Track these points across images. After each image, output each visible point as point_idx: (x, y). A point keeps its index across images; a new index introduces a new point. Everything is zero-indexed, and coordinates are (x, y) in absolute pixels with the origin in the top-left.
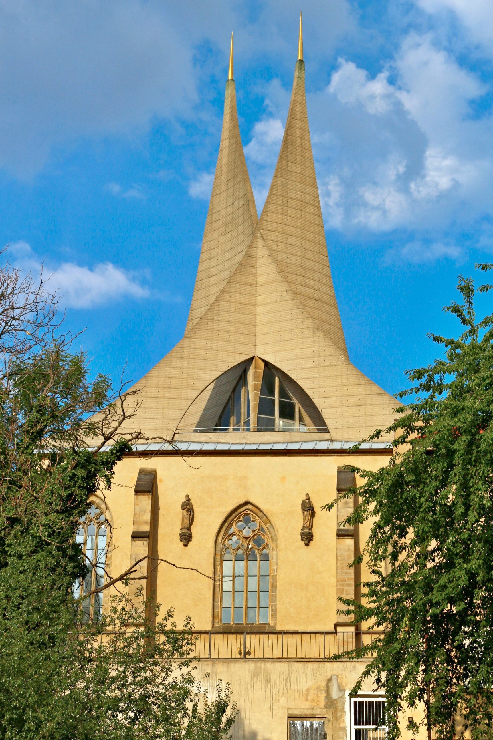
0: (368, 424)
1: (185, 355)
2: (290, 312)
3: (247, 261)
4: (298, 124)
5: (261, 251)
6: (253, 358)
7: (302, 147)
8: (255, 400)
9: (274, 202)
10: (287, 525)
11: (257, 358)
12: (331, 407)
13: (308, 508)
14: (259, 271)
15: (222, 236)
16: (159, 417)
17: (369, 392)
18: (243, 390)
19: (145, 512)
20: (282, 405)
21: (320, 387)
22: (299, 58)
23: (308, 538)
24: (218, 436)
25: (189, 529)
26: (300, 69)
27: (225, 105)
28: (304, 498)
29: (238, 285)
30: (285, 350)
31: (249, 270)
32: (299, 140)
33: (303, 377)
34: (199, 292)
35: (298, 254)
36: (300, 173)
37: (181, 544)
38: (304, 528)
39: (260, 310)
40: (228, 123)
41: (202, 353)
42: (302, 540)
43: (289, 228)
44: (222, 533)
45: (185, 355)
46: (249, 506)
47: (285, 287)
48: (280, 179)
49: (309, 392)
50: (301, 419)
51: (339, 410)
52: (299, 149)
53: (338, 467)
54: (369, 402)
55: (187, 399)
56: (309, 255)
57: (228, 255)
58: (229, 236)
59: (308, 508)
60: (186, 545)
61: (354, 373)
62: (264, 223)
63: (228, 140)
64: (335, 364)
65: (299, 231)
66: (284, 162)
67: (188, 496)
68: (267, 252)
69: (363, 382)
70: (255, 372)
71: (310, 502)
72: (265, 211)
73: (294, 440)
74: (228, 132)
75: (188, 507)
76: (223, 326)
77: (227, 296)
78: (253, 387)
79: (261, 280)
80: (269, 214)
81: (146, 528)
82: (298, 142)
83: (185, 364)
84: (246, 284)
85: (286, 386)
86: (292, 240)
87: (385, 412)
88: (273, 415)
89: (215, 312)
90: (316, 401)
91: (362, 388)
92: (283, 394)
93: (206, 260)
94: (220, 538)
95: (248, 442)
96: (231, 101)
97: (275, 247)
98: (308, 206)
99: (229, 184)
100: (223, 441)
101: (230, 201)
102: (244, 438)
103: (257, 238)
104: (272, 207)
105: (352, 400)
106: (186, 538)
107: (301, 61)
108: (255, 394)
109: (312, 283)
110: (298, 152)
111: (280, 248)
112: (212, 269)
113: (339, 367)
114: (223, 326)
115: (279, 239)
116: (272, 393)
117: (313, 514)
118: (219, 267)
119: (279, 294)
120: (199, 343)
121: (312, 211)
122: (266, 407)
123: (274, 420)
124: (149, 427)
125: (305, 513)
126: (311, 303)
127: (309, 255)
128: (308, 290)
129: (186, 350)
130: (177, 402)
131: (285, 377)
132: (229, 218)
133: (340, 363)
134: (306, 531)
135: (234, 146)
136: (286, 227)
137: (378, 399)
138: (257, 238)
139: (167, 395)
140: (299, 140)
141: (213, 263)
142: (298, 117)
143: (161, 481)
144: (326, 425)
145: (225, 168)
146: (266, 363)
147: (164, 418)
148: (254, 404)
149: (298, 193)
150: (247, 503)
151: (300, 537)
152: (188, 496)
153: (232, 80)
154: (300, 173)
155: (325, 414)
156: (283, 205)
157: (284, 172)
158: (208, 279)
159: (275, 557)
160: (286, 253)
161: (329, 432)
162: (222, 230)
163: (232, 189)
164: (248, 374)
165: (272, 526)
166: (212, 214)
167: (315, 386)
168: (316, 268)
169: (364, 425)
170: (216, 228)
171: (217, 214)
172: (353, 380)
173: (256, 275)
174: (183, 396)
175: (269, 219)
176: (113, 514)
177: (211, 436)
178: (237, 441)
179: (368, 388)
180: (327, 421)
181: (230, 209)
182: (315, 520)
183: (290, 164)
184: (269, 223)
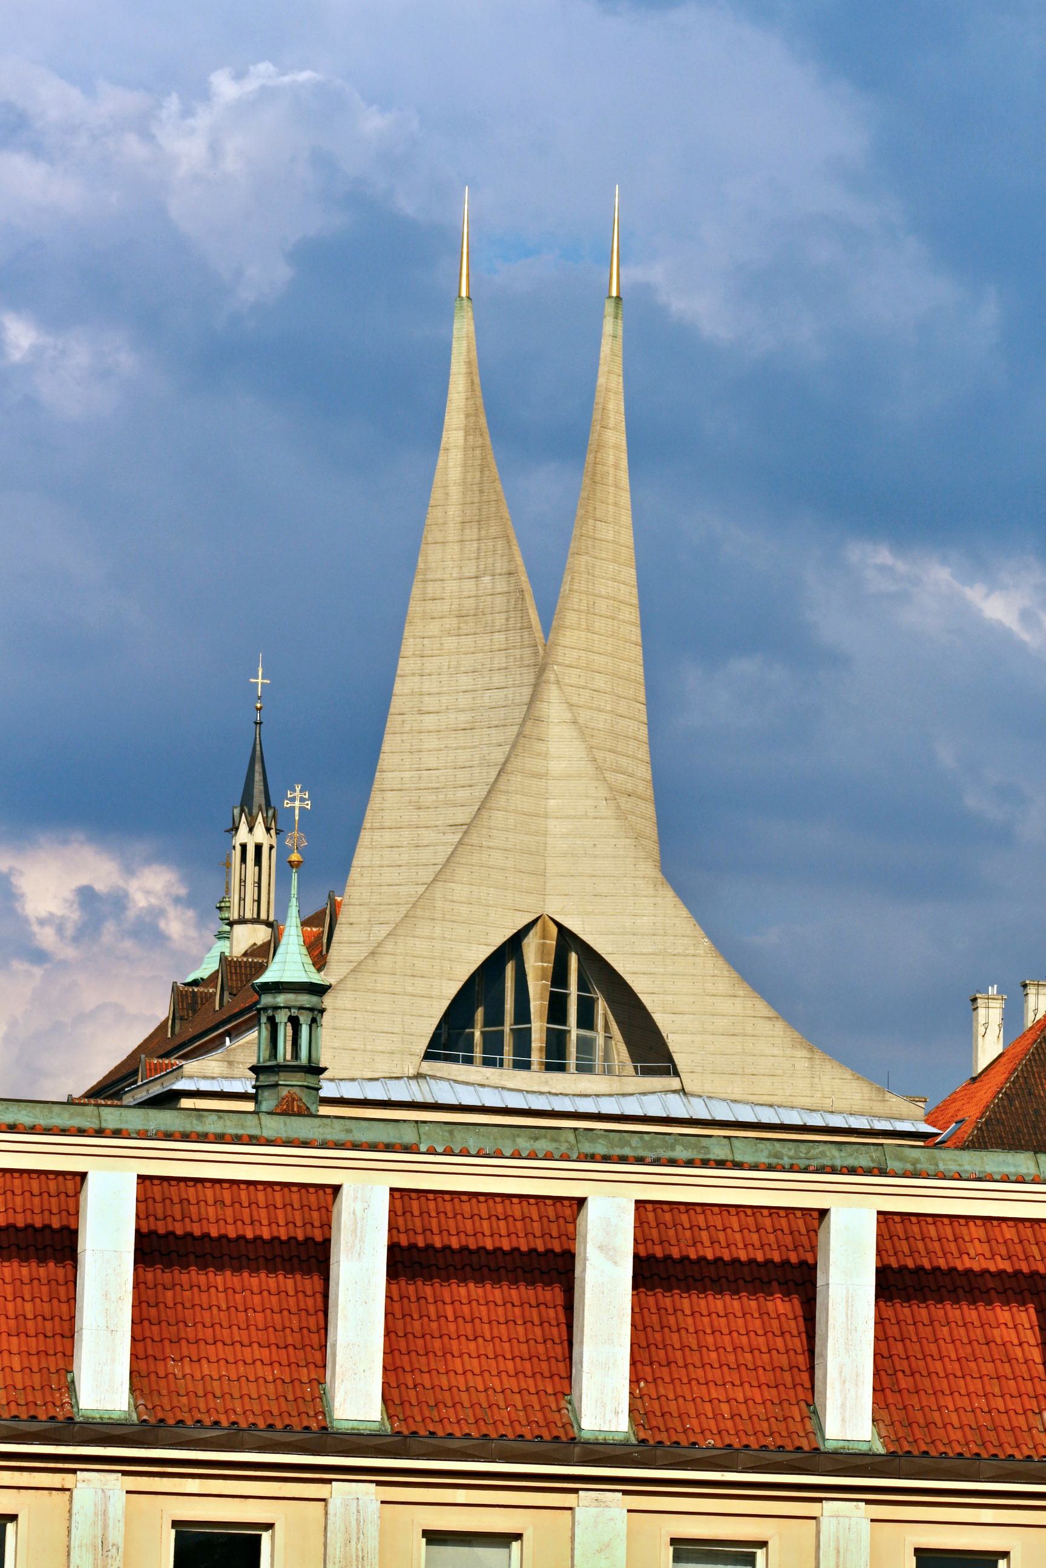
0: (747, 1071)
7: (616, 486)
9: (576, 607)
11: (547, 918)
12: (684, 1032)
15: (449, 635)
16: (396, 1030)
18: (510, 969)
21: (664, 993)
24: (501, 1075)
30: (603, 914)
32: (611, 470)
33: (635, 970)
34: (398, 738)
36: (614, 542)
39: (555, 826)
40: (463, 395)
43: (596, 657)
45: (438, 915)
47: (603, 793)
49: (645, 999)
54: (749, 1029)
55: (440, 998)
57: (465, 681)
58: (468, 641)
61: (726, 973)
63: (461, 433)
64: (692, 952)
66: (591, 521)
68: (568, 716)
69: (741, 993)
73: (626, 1091)
74: (462, 416)
78: (540, 972)
79: (556, 767)
82: (611, 479)
86: (600, 682)
87: (776, 1052)
89: (485, 831)
90: (657, 1017)
92: (582, 986)
93: (413, 674)
95: (553, 1091)
96: (469, 351)
97: (575, 699)
99: (467, 531)
101: (470, 569)
102: (547, 1083)
103: (548, 682)
107: (618, 298)
109: (624, 761)
110: (611, 500)
112: (426, 699)
113: (699, 960)
118: (444, 699)
120: (460, 891)
122: (557, 1010)
123: (569, 1031)
124: (380, 1048)
129: (439, 904)
131: (589, 954)
132: (469, 604)
133: (701, 952)
137: (765, 1027)
138: (548, 682)
139: (409, 989)
140: (611, 470)
141: (428, 685)
144: (671, 1060)
145: (455, 493)
147: (404, 1033)
148: (538, 1004)
154: (614, 542)
155: (674, 1042)
156: (588, 612)
158: (418, 717)
161: (677, 1074)
163: (475, 545)
164: (526, 942)
166: (425, 581)
167: (656, 990)
169: (740, 1071)
170: (435, 615)
173: (545, 756)
175: (567, 643)
177: (488, 1075)
178: (535, 1089)
179: (749, 1004)
181: (469, 586)
184: (567, 651)
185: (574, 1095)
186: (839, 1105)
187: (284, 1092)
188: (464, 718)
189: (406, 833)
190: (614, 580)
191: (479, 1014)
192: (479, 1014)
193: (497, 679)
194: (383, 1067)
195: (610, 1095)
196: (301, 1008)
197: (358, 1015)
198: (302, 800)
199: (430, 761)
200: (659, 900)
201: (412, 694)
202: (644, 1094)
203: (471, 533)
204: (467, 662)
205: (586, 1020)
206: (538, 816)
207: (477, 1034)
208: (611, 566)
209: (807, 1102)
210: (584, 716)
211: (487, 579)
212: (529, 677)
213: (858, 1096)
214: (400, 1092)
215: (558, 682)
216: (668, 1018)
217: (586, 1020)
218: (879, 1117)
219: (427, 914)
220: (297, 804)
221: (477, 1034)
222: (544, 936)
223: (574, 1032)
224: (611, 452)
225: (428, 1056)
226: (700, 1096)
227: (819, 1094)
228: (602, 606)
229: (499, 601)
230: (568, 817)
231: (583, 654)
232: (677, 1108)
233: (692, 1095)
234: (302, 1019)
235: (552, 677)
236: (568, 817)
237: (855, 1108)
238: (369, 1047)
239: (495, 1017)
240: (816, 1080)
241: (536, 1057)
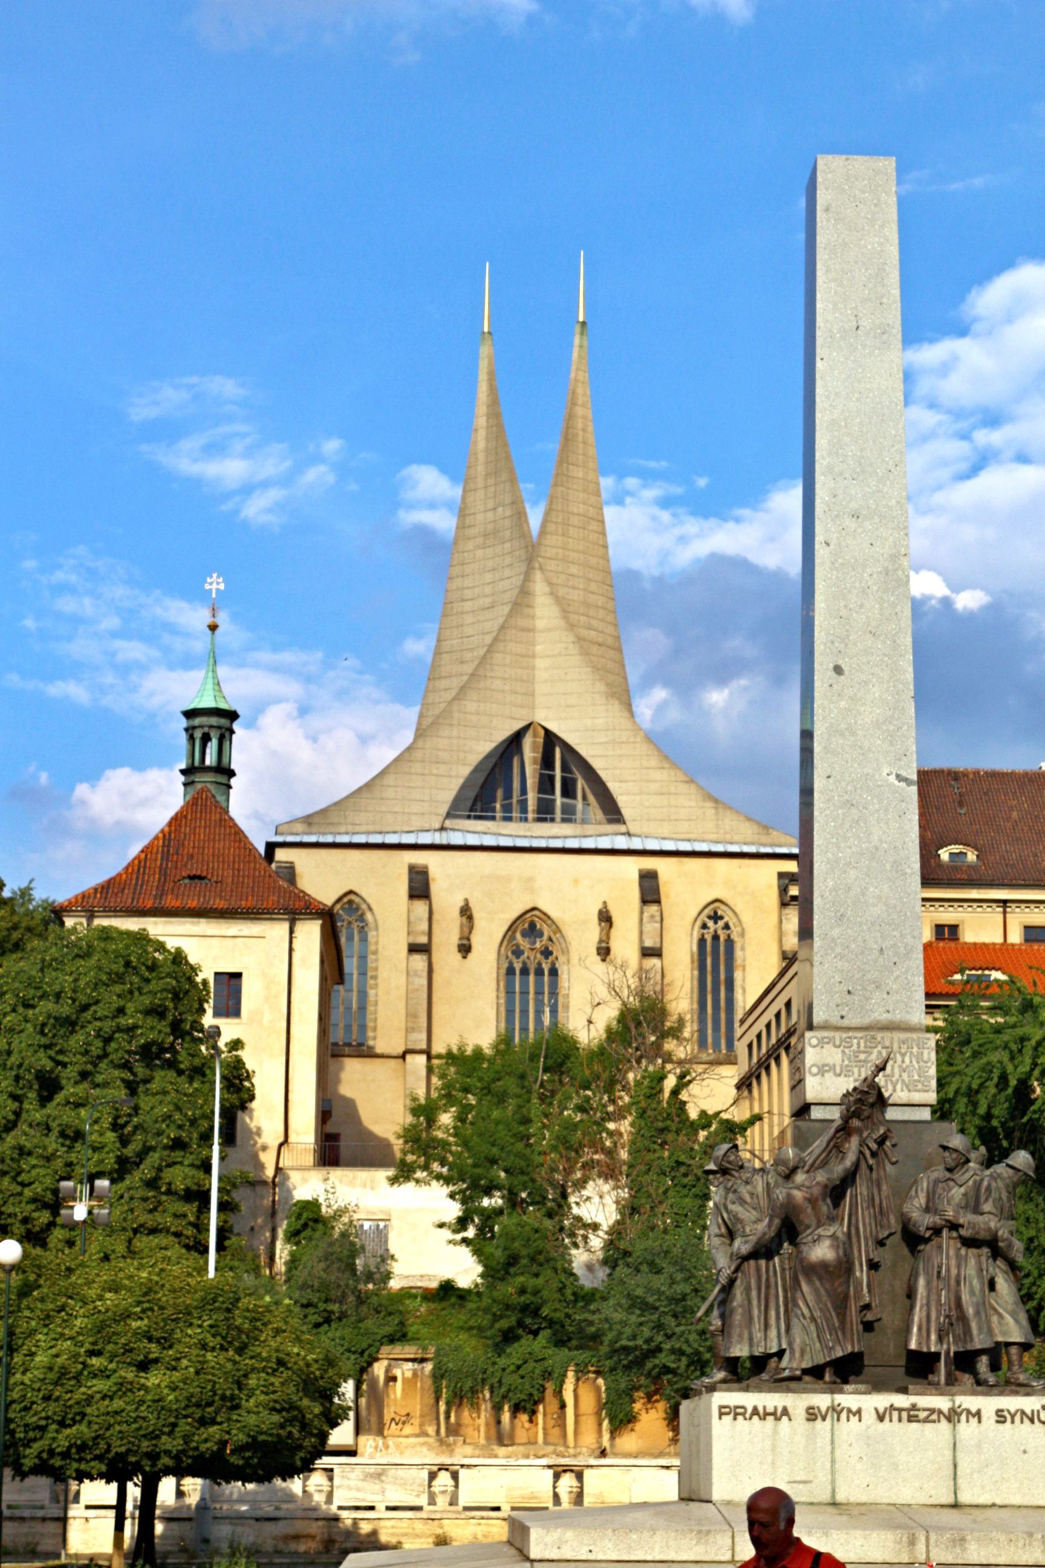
1: (455, 722)
2: (578, 670)
3: (522, 600)
5: (539, 586)
6: (529, 725)
8: (534, 777)
10: (582, 937)
12: (629, 794)
13: (605, 918)
14: (539, 611)
17: (673, 779)
19: (421, 920)
20: (564, 781)
21: (615, 768)
22: (581, 319)
23: (604, 952)
25: (469, 940)
26: (582, 334)
27: (481, 366)
28: (600, 906)
29: (513, 631)
31: (527, 611)
32: (580, 433)
35: (581, 587)
37: (459, 956)
38: (600, 941)
39: (540, 663)
40: (485, 394)
41: (474, 718)
42: (599, 954)
43: (571, 553)
44: (505, 943)
45: (455, 722)
46: (536, 913)
47: (571, 638)
48: (560, 489)
49: (603, 774)
50: (585, 798)
51: (638, 798)
52: (581, 445)
53: (640, 871)
54: (673, 789)
55: (457, 776)
56: (593, 587)
58: (489, 552)
59: (605, 918)
60: (465, 957)
62: (543, 548)
63: (484, 418)
65: (582, 556)
67: (466, 900)
68: (547, 589)
69: (667, 766)
70: (534, 743)
71: (607, 911)
72: (543, 532)
75: (466, 912)
76: (497, 684)
77: (501, 646)
79: (540, 624)
80: (548, 537)
81: (423, 940)
82: (580, 438)
83: (455, 733)
84: (523, 630)
85: (569, 758)
86: (574, 570)
88: (553, 792)
91: (665, 772)
92: (565, 768)
94: (503, 949)
97: (555, 580)
98: (592, 522)
100: (504, 832)
101: (491, 504)
102: (529, 830)
104: (551, 527)
105: (653, 787)
106: (465, 949)
107: (584, 324)
108: (535, 769)
109: (595, 623)
110: (580, 451)
111: (560, 581)
112: (466, 591)
113: (638, 745)
114: (497, 684)
115: (560, 569)
116: (553, 768)
117: (611, 926)
118: (476, 590)
119: (563, 645)
120: (470, 706)
121: (595, 528)
122: (546, 784)
123: (554, 801)
125: (603, 924)
126: (594, 649)
127: (593, 587)
128: (593, 633)
129: (456, 715)
130: (445, 780)
132: (490, 527)
134: (604, 945)
135: (494, 429)
136: (567, 553)
137: (683, 788)
139: (435, 771)
140: (580, 433)
141: (467, 582)
142: (580, 402)
143: (434, 880)
145: (481, 457)
146: (547, 732)
147: (431, 800)
148: (531, 782)
149: (581, 505)
150: (534, 909)
151: (595, 951)
152: (466, 900)
153: (489, 333)
155: (622, 801)
157: (564, 478)
159: (566, 972)
160: (567, 586)
161: (624, 823)
162: (480, 540)
165: (563, 936)
168: (600, 604)
171: (472, 517)
172: (654, 762)
173: (533, 617)
174: (453, 773)
176: (378, 917)
178: (521, 833)
179: (672, 773)
180: (624, 811)
181: (490, 515)
182: (613, 931)
183: (571, 467)
184: (548, 549)
185: (549, 837)
186: (736, 838)
187: (199, 786)
188: (488, 600)
189: (455, 680)
190: (584, 504)
191: (500, 793)
192: (500, 793)
193: (507, 572)
194: (417, 823)
195: (575, 837)
196: (211, 727)
197: (399, 789)
198: (218, 583)
199: (469, 631)
200: (610, 707)
201: (458, 589)
202: (600, 835)
203: (491, 481)
204: (490, 564)
205: (568, 791)
206: (528, 656)
207: (498, 806)
208: (581, 495)
209: (714, 837)
210: (561, 592)
211: (500, 509)
212: (523, 568)
213: (750, 832)
214: (425, 839)
215: (541, 568)
216: (617, 785)
217: (568, 791)
218: (765, 845)
219: (447, 721)
220: (214, 586)
221: (498, 806)
222: (535, 735)
223: (559, 800)
224: (580, 420)
225: (449, 815)
226: (639, 836)
227: (722, 831)
228: (575, 520)
229: (507, 522)
230: (548, 656)
231: (560, 551)
232: (621, 843)
233: (635, 835)
234: (212, 735)
235: (537, 565)
236: (548, 656)
237: (749, 840)
238: (406, 811)
239: (508, 795)
240: (720, 822)
241: (530, 816)
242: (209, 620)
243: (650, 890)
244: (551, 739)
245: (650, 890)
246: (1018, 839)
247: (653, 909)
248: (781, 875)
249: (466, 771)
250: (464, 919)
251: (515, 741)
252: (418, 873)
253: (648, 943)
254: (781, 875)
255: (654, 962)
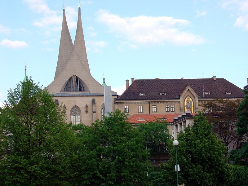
4: (80, 23)
10: (83, 110)
23: (87, 112)
59: (87, 107)
75: (65, 107)
151: (85, 111)
242: (25, 68)
243: (94, 102)
244: (77, 78)
245: (94, 102)
246: (152, 91)
247: (94, 105)
248: (114, 99)
249: (63, 83)
250: (64, 108)
251: (71, 79)
252: (57, 101)
253: (94, 111)
254: (114, 99)
255: (95, 113)
